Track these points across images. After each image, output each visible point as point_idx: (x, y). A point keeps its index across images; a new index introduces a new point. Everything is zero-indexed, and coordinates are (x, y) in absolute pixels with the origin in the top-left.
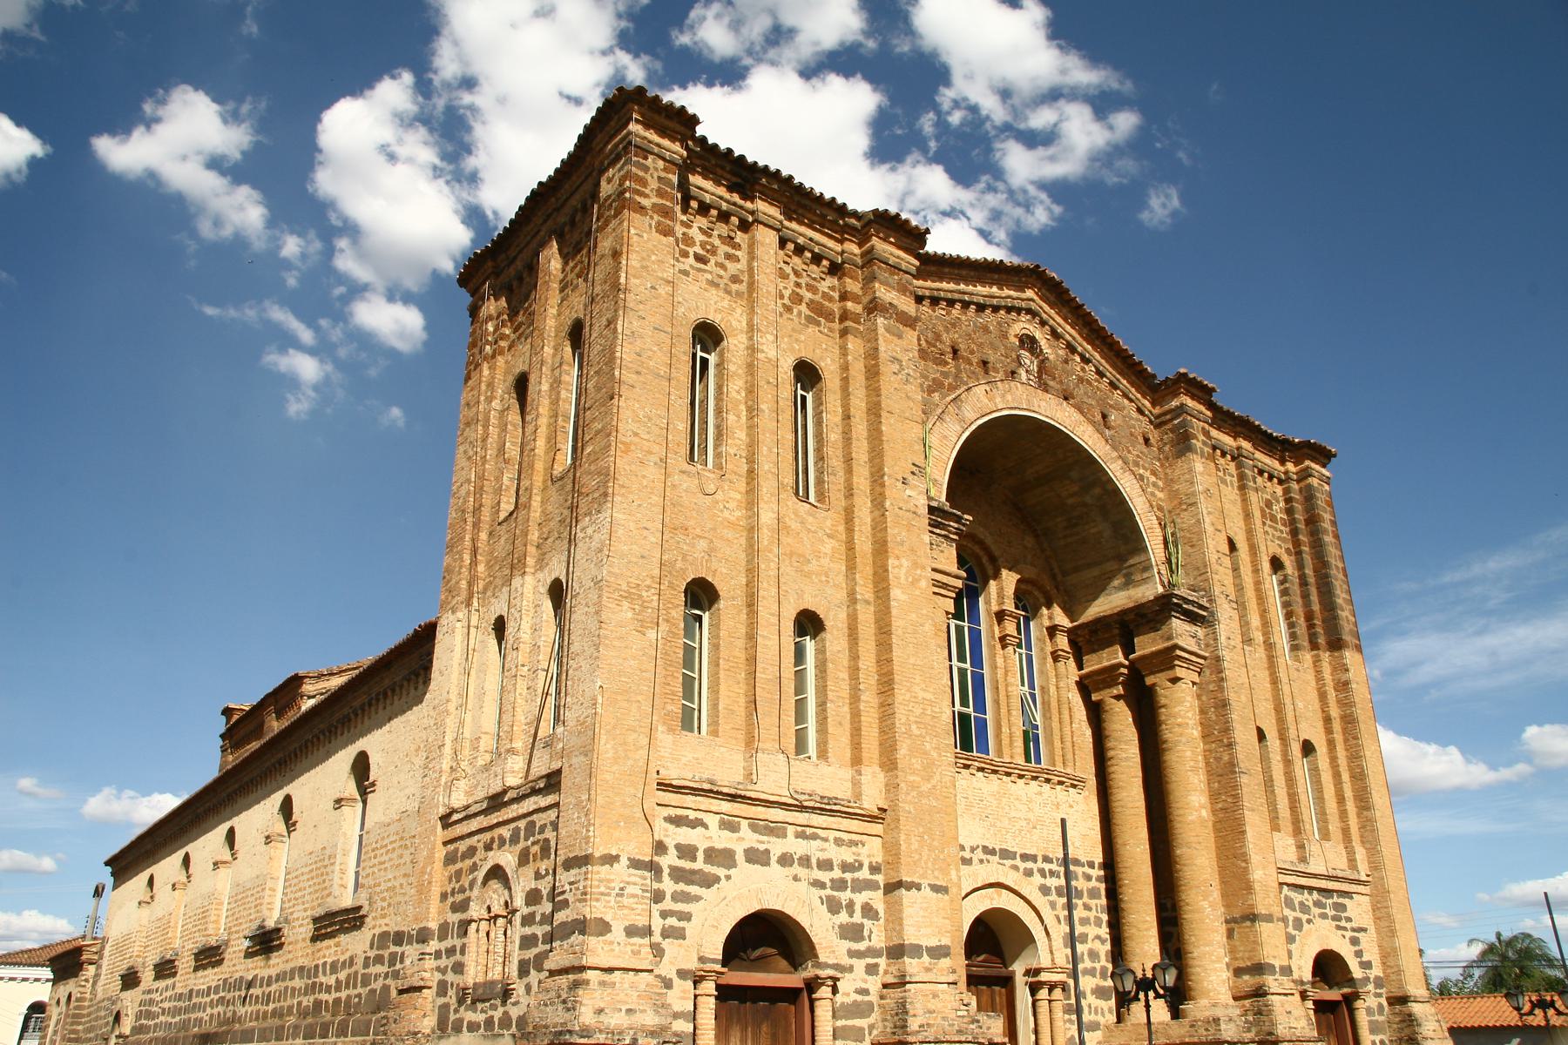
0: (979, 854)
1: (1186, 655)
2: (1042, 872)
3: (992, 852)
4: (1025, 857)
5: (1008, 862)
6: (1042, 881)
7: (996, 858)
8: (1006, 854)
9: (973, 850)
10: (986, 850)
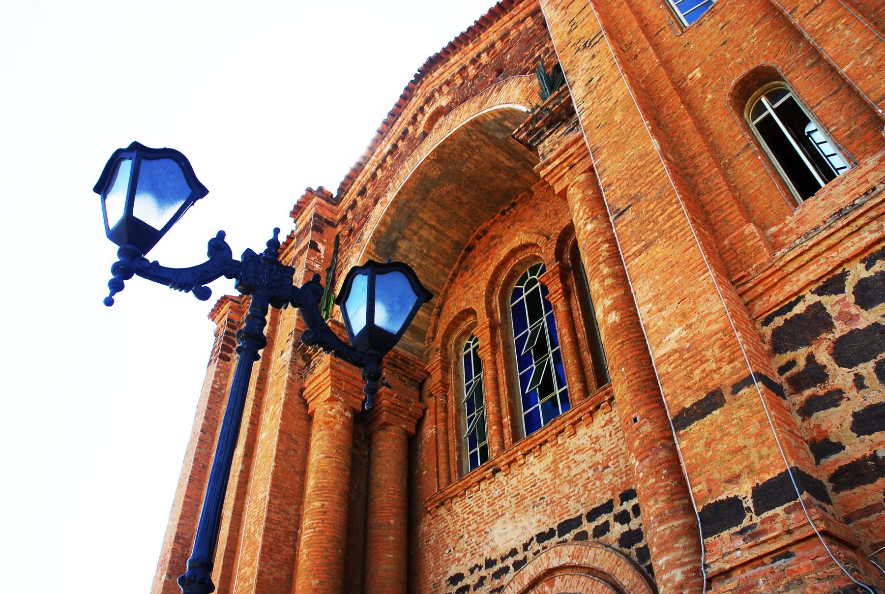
0: (536, 546)
1: (557, 162)
2: (623, 518)
3: (551, 534)
4: (592, 515)
5: (569, 536)
6: (625, 528)
7: (556, 539)
8: (565, 527)
9: (526, 547)
10: (542, 537)
